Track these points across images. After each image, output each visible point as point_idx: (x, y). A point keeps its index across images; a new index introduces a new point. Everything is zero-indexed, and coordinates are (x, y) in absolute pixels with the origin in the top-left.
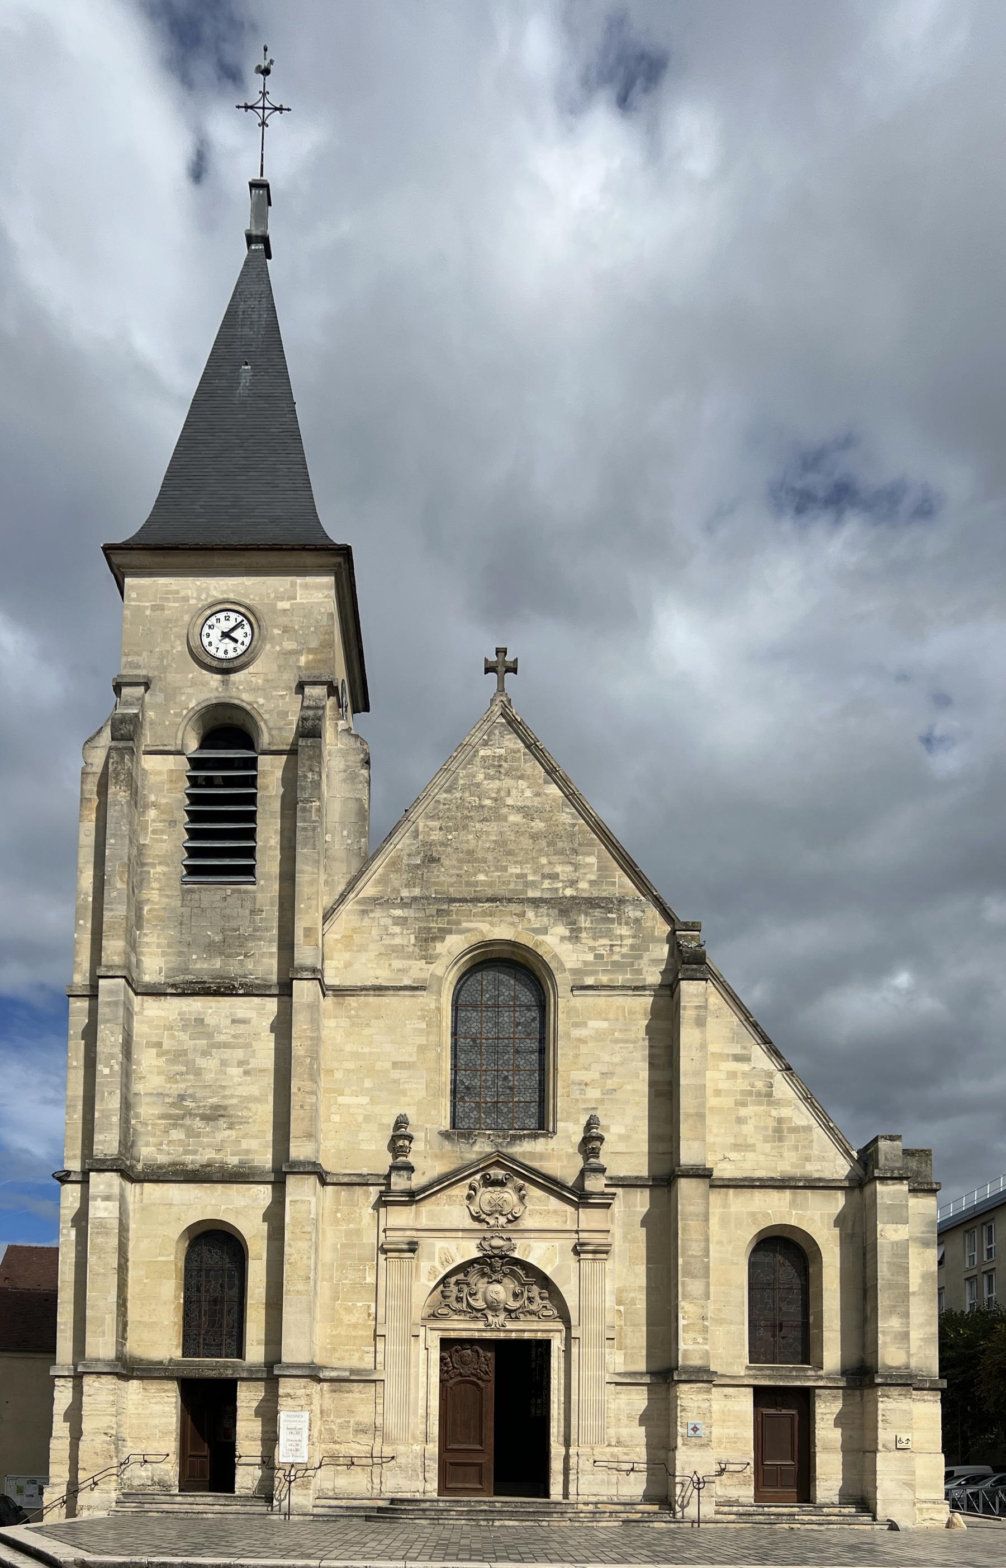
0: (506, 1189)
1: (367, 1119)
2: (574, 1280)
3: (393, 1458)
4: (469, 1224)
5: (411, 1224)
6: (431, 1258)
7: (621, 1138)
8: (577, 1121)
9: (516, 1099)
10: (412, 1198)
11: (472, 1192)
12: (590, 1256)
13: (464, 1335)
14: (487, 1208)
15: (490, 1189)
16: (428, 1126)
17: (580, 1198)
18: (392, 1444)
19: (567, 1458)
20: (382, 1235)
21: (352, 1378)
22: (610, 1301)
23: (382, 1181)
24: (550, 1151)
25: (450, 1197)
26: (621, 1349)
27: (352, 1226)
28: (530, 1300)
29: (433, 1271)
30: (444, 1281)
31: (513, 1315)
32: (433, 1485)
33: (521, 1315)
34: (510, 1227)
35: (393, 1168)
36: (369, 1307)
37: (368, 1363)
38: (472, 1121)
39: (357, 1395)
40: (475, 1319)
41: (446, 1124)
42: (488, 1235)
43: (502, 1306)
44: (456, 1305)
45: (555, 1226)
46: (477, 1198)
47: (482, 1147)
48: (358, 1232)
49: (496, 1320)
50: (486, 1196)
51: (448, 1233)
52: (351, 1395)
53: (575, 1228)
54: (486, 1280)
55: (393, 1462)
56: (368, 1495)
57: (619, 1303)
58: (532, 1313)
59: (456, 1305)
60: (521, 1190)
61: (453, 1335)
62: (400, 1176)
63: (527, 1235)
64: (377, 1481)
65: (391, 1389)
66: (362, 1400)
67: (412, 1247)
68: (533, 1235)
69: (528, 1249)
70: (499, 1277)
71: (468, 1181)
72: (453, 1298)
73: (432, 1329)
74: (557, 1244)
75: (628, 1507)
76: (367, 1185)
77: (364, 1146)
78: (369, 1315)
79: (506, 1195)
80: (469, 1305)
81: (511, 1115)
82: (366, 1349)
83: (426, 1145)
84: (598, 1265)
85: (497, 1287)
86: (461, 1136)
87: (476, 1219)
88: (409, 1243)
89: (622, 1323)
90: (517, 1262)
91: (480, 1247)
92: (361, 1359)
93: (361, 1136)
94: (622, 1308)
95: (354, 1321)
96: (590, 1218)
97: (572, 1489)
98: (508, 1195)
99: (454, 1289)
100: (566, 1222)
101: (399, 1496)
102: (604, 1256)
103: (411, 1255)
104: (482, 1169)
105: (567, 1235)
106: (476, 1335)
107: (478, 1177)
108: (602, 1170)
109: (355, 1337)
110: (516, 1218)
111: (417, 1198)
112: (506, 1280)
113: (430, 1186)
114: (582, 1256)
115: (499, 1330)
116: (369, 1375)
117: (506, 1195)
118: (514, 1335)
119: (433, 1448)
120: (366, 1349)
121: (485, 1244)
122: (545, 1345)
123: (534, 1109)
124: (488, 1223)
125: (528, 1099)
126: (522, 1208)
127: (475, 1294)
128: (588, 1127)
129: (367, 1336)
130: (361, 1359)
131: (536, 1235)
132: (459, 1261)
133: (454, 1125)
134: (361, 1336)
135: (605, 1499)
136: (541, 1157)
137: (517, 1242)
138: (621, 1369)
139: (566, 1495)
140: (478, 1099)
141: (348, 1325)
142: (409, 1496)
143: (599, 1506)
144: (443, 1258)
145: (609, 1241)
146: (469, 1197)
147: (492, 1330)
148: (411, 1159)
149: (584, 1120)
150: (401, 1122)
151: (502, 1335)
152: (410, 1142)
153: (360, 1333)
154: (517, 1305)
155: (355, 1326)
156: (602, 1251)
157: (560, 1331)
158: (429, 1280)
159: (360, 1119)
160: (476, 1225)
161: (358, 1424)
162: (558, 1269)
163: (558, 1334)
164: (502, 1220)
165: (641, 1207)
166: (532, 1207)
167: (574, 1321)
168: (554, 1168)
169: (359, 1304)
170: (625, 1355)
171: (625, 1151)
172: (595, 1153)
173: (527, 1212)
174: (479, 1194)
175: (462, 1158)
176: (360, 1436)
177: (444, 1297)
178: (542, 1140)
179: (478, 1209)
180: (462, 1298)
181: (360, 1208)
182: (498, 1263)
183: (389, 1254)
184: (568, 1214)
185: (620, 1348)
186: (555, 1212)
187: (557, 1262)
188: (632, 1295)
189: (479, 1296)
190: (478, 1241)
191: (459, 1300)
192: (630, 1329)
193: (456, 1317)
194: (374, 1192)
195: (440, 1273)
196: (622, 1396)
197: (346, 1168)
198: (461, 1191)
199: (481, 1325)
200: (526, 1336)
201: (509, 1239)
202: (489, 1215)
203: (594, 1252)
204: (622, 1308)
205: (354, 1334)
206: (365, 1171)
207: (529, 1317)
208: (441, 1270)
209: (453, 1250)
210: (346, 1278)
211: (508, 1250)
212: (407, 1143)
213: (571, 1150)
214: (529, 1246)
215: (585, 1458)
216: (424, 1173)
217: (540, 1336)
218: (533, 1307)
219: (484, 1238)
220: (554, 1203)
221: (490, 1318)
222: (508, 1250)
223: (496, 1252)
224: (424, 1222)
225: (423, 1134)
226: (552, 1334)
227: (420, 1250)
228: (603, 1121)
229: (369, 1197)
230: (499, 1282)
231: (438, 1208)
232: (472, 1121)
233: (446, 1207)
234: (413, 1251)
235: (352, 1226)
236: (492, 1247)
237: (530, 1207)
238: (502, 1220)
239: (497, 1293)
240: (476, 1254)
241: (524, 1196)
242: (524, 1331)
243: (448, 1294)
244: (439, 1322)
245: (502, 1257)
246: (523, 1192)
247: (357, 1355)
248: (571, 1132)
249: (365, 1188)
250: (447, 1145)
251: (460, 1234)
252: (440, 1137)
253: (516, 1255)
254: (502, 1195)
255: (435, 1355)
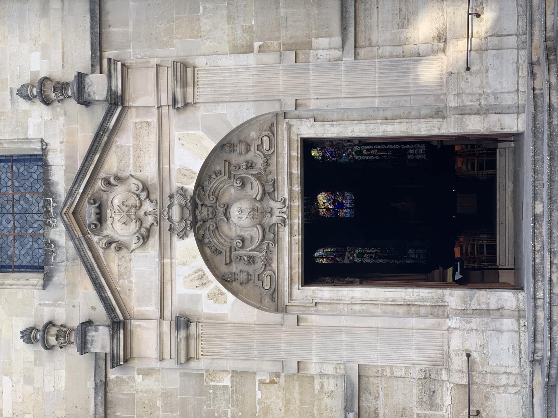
0: (109, 203)
1: (28, 380)
2: (221, 110)
3: (468, 355)
4: (153, 248)
5: (153, 324)
6: (196, 299)
7: (44, 57)
8: (27, 113)
9: (10, 190)
10: (118, 324)
11: (113, 245)
12: (190, 90)
13: (297, 254)
14: (133, 227)
15: (109, 222)
16: (36, 303)
17: (116, 105)
18: (449, 355)
19: (463, 111)
20: (166, 364)
21: (356, 410)
22: (249, 59)
23: (102, 363)
24: (63, 146)
25: (120, 275)
26: (310, 43)
27: (159, 403)
28: (250, 165)
29: (214, 297)
30: (226, 280)
31: (270, 189)
32: (507, 298)
33: (270, 177)
34: (155, 196)
35: (83, 348)
36: (262, 382)
37: (335, 387)
38: (36, 245)
39: (381, 403)
40: (276, 240)
41: (36, 279)
42: (167, 224)
43: (258, 205)
44: (259, 264)
45: (153, 137)
46: (121, 239)
47: (58, 234)
48: (166, 395)
49: (276, 212)
50: (118, 227)
51: (169, 276)
52: (381, 412)
53: (155, 111)
54: (225, 227)
55: (474, 354)
56: (527, 391)
57: (249, 50)
58: (267, 164)
59: (259, 264)
60: (109, 183)
61: (298, 270)
62: (92, 341)
63: (166, 174)
64: (504, 380)
65: (371, 358)
66: (386, 395)
67: (183, 323)
68: (166, 166)
69: (184, 172)
70: (221, 210)
71: (101, 251)
72: (250, 269)
73: (290, 298)
74: (176, 134)
75: (537, 16)
76: (106, 383)
77: (62, 385)
78: (272, 382)
79: (116, 202)
80: (258, 249)
81: (29, 197)
82: (317, 387)
83: (59, 306)
84: (202, 79)
85: (234, 211)
86: (47, 261)
87: (144, 239)
88: (178, 329)
89: (276, 43)
90: (199, 185)
91: (183, 235)
92: (331, 395)
93: (49, 388)
94: (256, 45)
95: (280, 403)
96: (144, 92)
97: (509, 100)
98: (117, 197)
99: (235, 268)
100: (148, 124)
101: (525, 347)
102: (189, 71)
103: (193, 326)
104: (84, 234)
105: (165, 121)
106: (298, 238)
107: (95, 239)
108: (81, 77)
109: (302, 402)
110: (145, 188)
111: (121, 318)
112: (225, 199)
113: (104, 300)
114: (190, 100)
115: (290, 208)
116: (352, 385)
117: (116, 202)
118: (297, 188)
119: (454, 297)
120: (317, 387)
121: (179, 227)
122: (308, 144)
123: (19, 168)
124: (152, 224)
125: (10, 176)
126: (133, 181)
127: (243, 240)
128: (29, 98)
129: (301, 386)
130: (331, 395)
131: (165, 161)
132: (200, 262)
133: (38, 269)
134: (301, 393)
135: (523, 54)
136: (70, 157)
137: (176, 185)
138: (337, 40)
139: (518, 110)
140: (11, 238)
141: (287, 411)
142: (525, 336)
143: (534, 59)
144: (197, 283)
145: (170, 64)
146: (119, 249)
147: (290, 217)
148: (75, 323)
149: (23, 104)
150: (28, 336)
151: (297, 204)
152: (54, 325)
153: (296, 395)
154: (256, 183)
155: (288, 402)
156: (183, 72)
157: (289, 127)
158: (225, 302)
159: (29, 389)
160: (154, 241)
161: (421, 403)
162: (208, 131)
163: (294, 130)
164: (148, 207)
165: (127, 25)
166: (131, 168)
167: (276, 108)
168: (84, 139)
169: (259, 395)
170: (318, 37)
171: (60, 51)
172: (61, 87)
173: (137, 174)
174: (116, 237)
175: (74, 259)
176: (438, 401)
177: (249, 280)
178: (51, 158)
179: (135, 240)
180: (250, 257)
181: (137, 392)
182: (203, 213)
183: (193, 355)
184: (139, 120)
185: (309, 46)
186: (137, 137)
187: (200, 133)
188: (239, 32)
189: (246, 234)
190: (175, 238)
191: (251, 260)
192: (283, 32)
193: (274, 265)
194: (113, 374)
195: (216, 288)
196: (374, 38)
197: (88, 410)
198: (113, 261)
199: (284, 232)
200: (297, 171)
201: (171, 197)
202: (141, 224)
203: (184, 85)
204: (256, 45)
205: (298, 404)
206: (91, 384)
207: (273, 167)
208: (212, 286)
209: (187, 270)
210: (225, 412)
211: (186, 199)
212: (54, 331)
213: (62, 120)
214: (179, 170)
215: (463, 84)
216: (94, 308)
217: (296, 153)
218: (260, 162)
219: (171, 229)
220: (124, 140)
221: (274, 220)
222: (186, 199)
223: (187, 213)
224: (152, 309)
225: (46, 309)
226: (294, 137)
227: (187, 313)
228: (26, 79)
229: (123, 380)
230: (227, 207)
231: (135, 290)
232: (36, 245)
233: (133, 279)
234: (188, 323)
235: (159, 403)
236: (182, 218)
237: (131, 170)
238: (148, 207)
239: (241, 211)
240: (191, 241)
241: (118, 178)
242: (290, 175)
243: (244, 277)
244: (281, 288)
245: (195, 206)
246: (112, 180)
247: (327, 401)
248: (39, 120)
249: (111, 385)
250: (59, 277)
251: (167, 261)
252: (49, 288)
253: (191, 187)
254: (116, 207)
255: (324, 292)
